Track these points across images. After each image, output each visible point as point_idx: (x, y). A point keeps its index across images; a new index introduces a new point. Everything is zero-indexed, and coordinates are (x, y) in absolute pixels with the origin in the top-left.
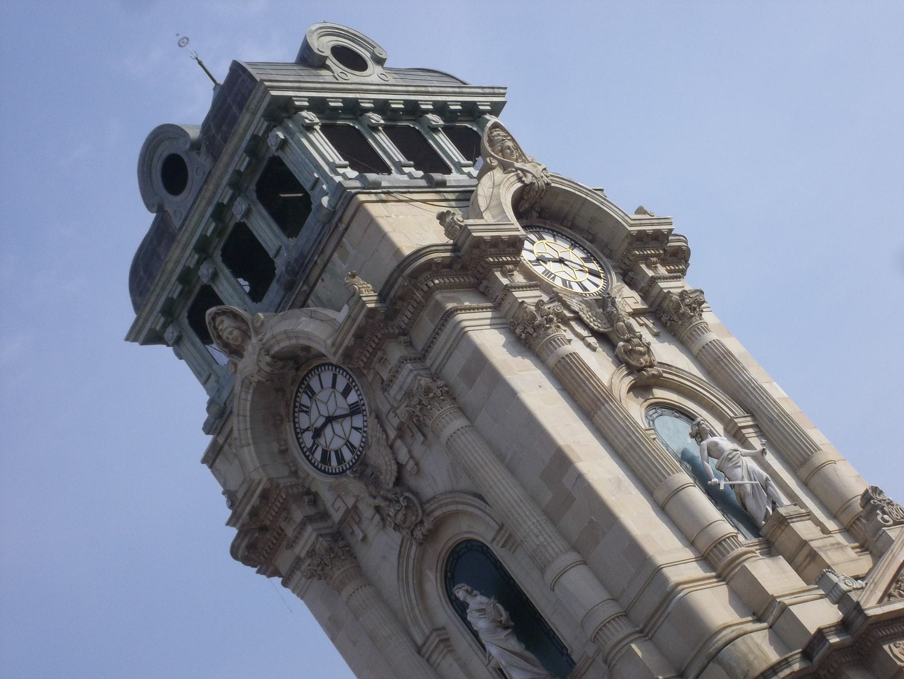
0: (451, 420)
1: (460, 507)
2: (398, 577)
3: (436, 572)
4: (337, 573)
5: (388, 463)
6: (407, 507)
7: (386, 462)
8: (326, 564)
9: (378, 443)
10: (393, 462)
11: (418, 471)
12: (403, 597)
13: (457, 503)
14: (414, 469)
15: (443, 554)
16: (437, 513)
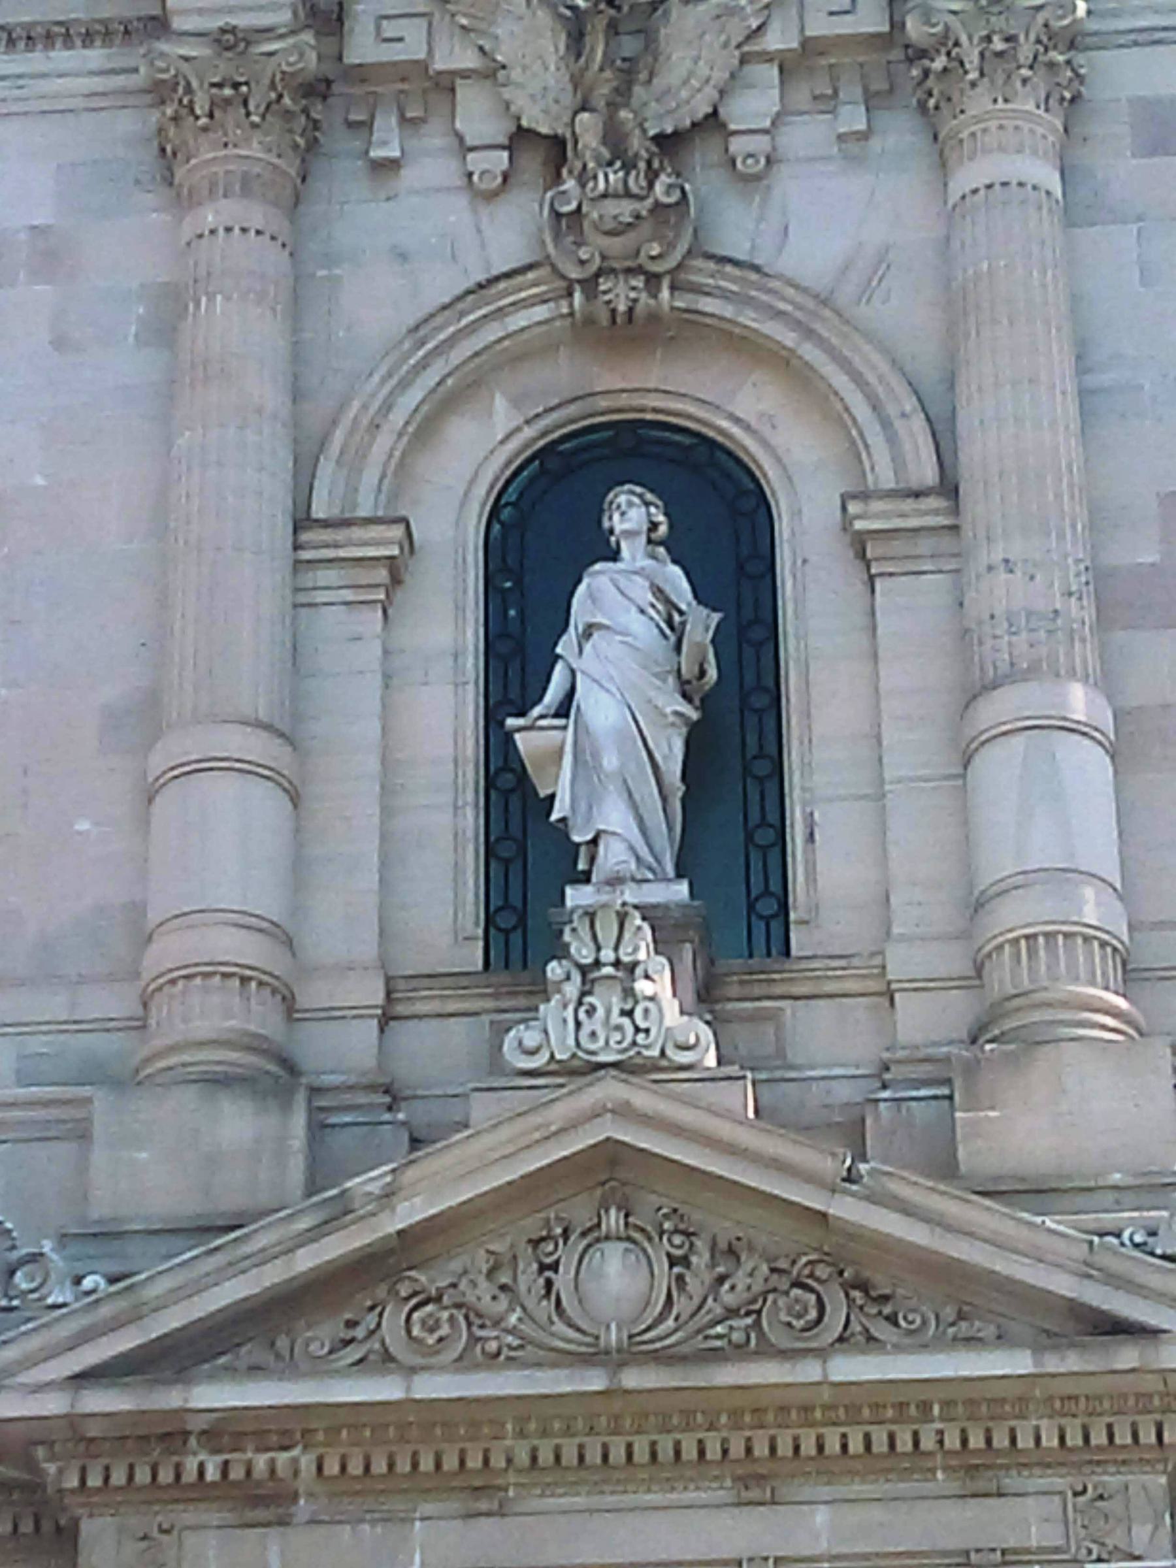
0: (1035, 153)
1: (810, 352)
2: (417, 328)
3: (528, 422)
4: (254, 149)
5: (694, 83)
6: (658, 206)
7: (691, 74)
8: (245, 103)
9: (718, 17)
10: (710, 93)
11: (757, 178)
12: (376, 378)
13: (809, 333)
14: (750, 161)
15: (603, 403)
16: (708, 305)
